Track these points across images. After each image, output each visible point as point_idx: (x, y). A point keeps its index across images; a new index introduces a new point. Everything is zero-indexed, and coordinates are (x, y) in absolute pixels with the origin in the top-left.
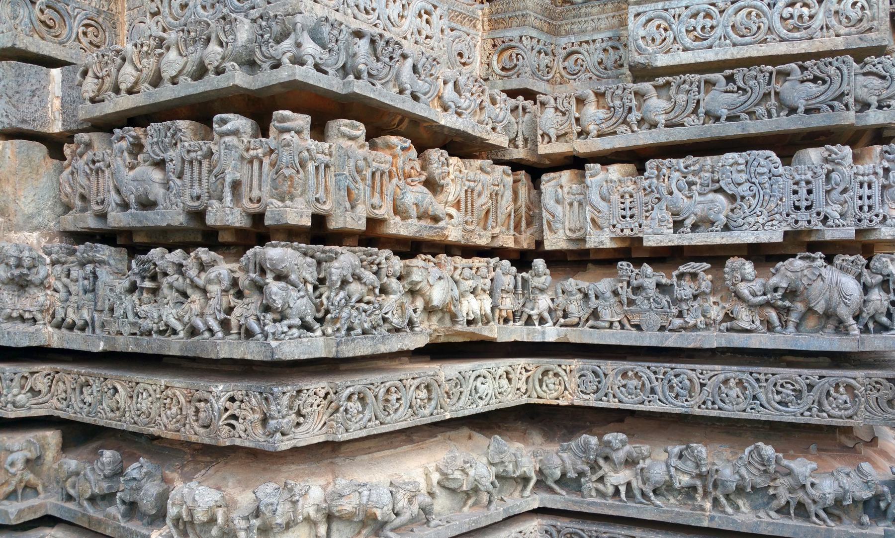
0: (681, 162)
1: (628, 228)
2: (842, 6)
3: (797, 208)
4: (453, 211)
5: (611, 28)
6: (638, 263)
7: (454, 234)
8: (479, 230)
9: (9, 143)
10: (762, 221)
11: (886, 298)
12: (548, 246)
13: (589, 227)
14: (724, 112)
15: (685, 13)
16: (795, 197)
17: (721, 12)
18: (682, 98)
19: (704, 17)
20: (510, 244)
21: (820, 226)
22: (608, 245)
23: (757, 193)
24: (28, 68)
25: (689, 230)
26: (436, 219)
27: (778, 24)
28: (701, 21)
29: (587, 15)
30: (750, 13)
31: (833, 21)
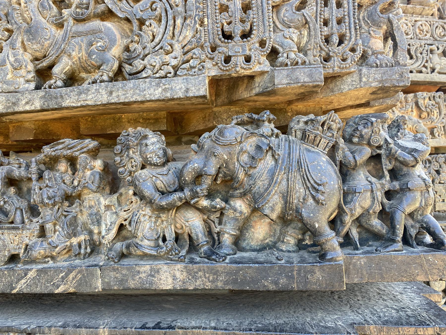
3: (228, 37)
10: (174, 62)
11: (379, 186)
16: (224, 18)
21: (266, 66)
23: (164, 14)
25: (60, 83)
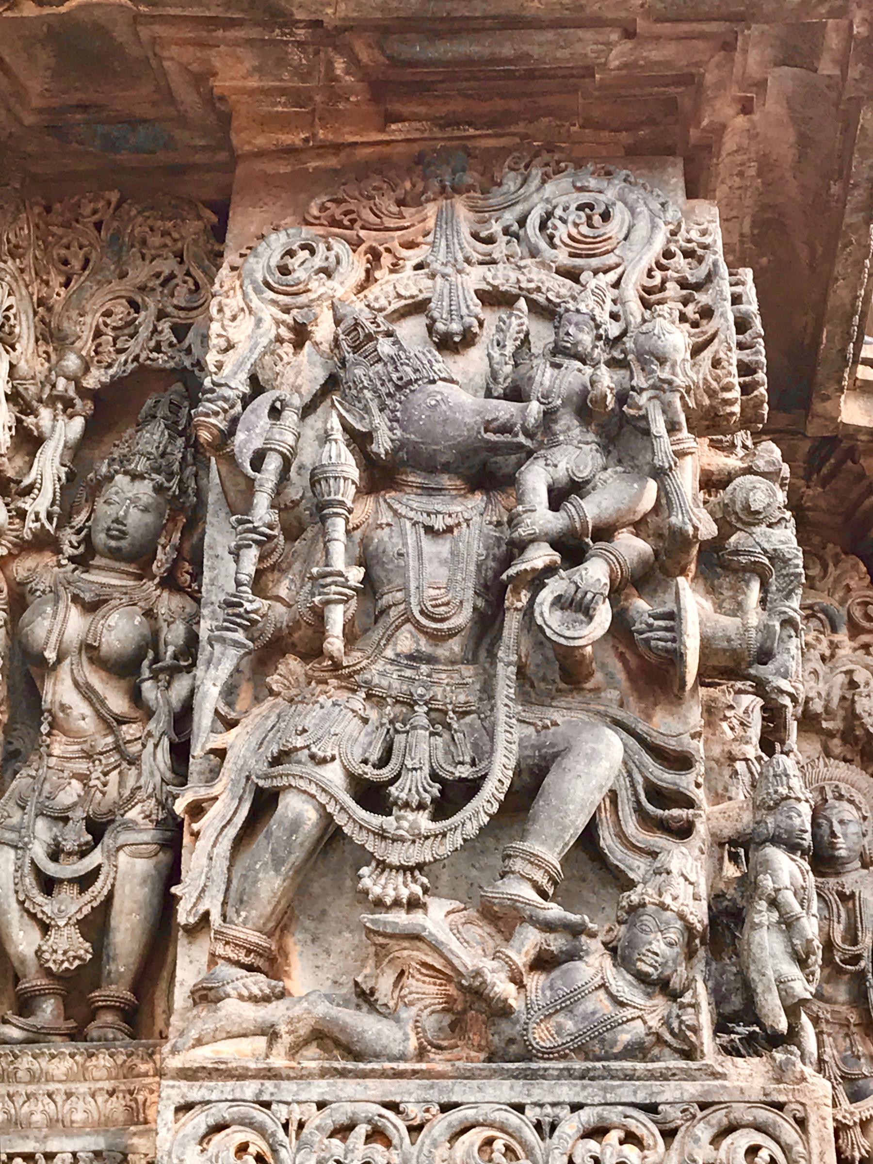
2: (722, 1154)
5: (102, 1125)
17: (415, 1130)
19: (369, 1138)
29: (34, 1078)
30: (489, 1142)
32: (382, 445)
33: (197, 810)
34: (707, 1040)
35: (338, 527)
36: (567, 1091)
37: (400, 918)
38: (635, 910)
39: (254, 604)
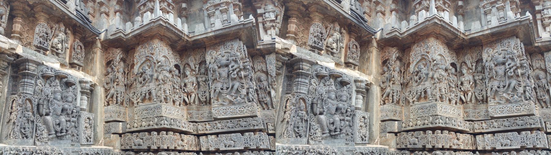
0: (501, 134)
1: (493, 146)
4: (461, 144)
6: (495, 152)
7: (462, 148)
8: (466, 147)
9: (390, 134)
12: (479, 149)
13: (486, 146)
14: (507, 126)
15: (498, 108)
18: (500, 123)
20: (472, 149)
22: (490, 149)
24: (393, 122)
26: (459, 145)
27: (515, 110)
28: (501, 109)
31: (524, 110)
32: (496, 64)
33: (488, 89)
34: (524, 100)
35: (493, 70)
36: (514, 104)
37: (502, 95)
38: (518, 92)
39: (489, 76)
